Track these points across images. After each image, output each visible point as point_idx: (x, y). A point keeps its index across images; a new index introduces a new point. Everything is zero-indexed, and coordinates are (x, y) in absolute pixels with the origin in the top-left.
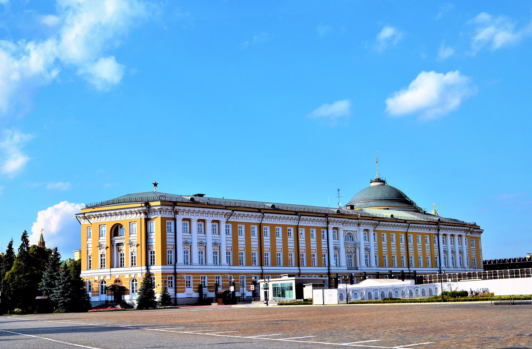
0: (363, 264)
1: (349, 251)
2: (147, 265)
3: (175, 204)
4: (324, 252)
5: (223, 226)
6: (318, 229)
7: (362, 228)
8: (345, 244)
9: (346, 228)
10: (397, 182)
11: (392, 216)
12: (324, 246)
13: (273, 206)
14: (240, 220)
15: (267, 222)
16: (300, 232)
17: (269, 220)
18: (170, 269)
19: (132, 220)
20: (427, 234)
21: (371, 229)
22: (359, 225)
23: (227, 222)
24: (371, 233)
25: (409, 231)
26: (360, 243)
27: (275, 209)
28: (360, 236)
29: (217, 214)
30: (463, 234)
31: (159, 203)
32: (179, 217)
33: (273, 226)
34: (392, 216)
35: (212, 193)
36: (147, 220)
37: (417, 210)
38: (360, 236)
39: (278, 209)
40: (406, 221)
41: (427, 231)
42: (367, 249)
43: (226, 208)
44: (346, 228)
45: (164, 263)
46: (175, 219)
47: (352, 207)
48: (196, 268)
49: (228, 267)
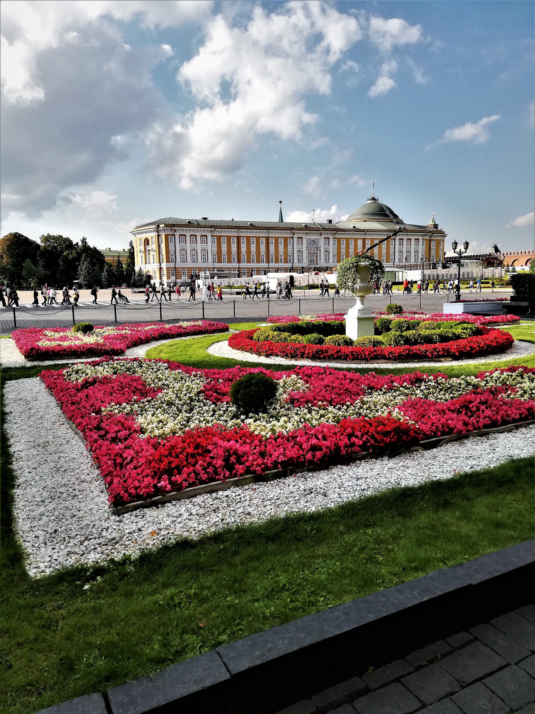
0: (322, 261)
1: (312, 252)
2: (160, 262)
3: (174, 225)
4: (290, 253)
5: (209, 238)
6: (286, 239)
7: (323, 236)
8: (307, 248)
10: (384, 201)
11: (354, 227)
12: (392, 251)
13: (251, 224)
16: (367, 241)
17: (244, 233)
18: (172, 265)
19: (152, 236)
21: (331, 237)
22: (321, 235)
24: (331, 241)
25: (367, 237)
26: (320, 247)
27: (252, 227)
28: (322, 242)
29: (204, 231)
30: (421, 238)
31: (163, 225)
32: (177, 234)
33: (248, 238)
34: (354, 227)
35: (214, 216)
36: (159, 236)
37: (400, 222)
38: (322, 242)
39: (255, 226)
40: (364, 230)
42: (327, 251)
43: (211, 227)
45: (168, 261)
47: (330, 221)
48: (189, 264)
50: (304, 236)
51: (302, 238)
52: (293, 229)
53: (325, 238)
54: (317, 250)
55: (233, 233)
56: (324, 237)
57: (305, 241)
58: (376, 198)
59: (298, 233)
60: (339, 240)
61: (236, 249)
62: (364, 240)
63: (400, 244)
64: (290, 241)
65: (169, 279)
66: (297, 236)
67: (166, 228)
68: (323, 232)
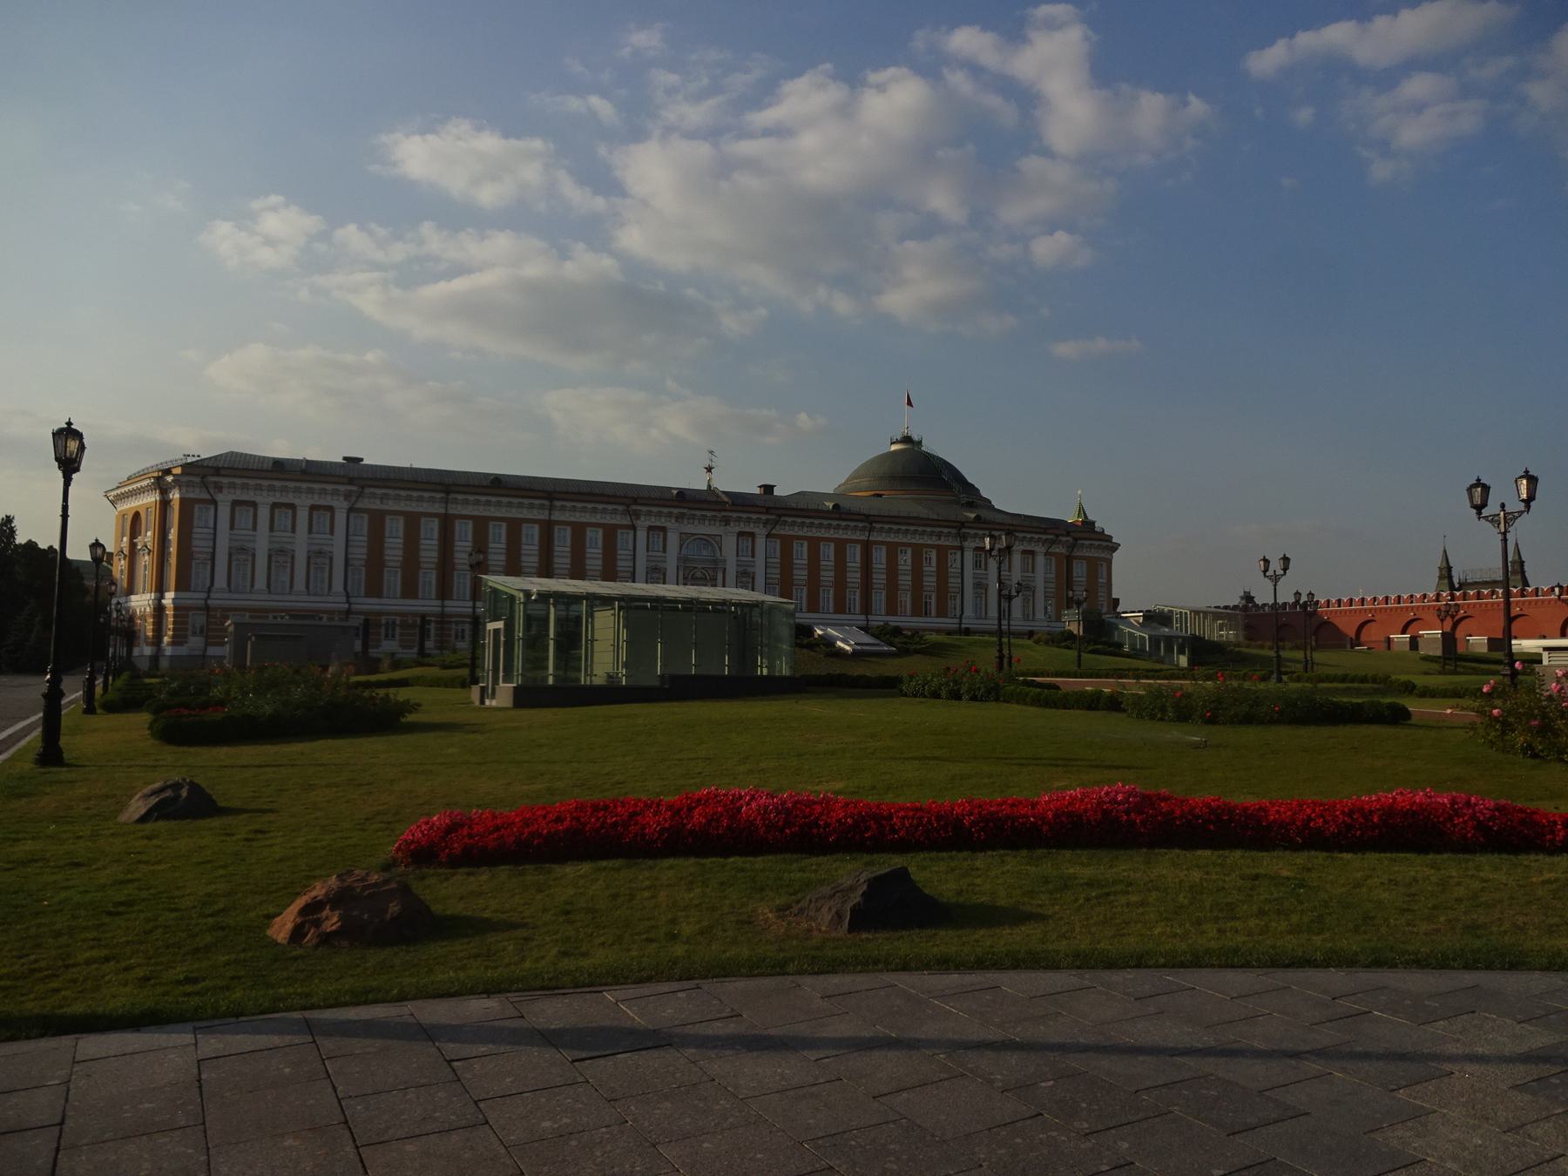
1: (699, 575)
7: (735, 528)
9: (689, 528)
14: (391, 505)
15: (563, 518)
20: (932, 546)
22: (727, 521)
23: (351, 510)
25: (875, 537)
41: (933, 541)
44: (689, 528)
46: (634, 528)
49: (227, 595)
50: (670, 524)
51: (664, 529)
52: (635, 501)
53: (740, 534)
54: (715, 570)
55: (431, 506)
56: (737, 529)
57: (673, 539)
58: (916, 438)
59: (649, 513)
60: (787, 543)
61: (435, 554)
62: (867, 547)
63: (977, 565)
64: (624, 538)
65: (181, 644)
66: (648, 523)
67: (184, 479)
68: (735, 515)
